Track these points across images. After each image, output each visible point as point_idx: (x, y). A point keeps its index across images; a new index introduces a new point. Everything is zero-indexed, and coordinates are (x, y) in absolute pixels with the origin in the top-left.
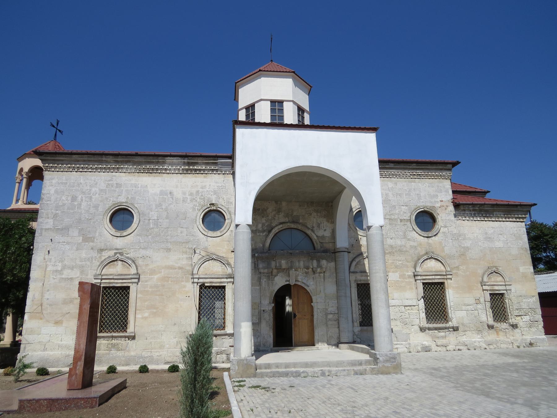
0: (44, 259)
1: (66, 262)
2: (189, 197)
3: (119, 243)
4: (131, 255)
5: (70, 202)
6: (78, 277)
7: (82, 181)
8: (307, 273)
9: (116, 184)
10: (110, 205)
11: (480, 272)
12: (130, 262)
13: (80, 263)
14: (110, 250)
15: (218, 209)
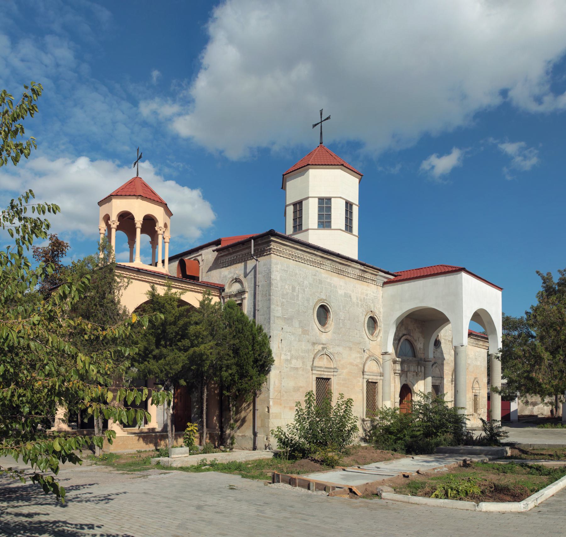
0: (279, 348)
1: (292, 352)
2: (360, 302)
3: (324, 338)
4: (331, 350)
5: (291, 291)
6: (301, 368)
7: (297, 272)
8: (414, 375)
9: (319, 280)
10: (317, 300)
11: (472, 381)
12: (332, 357)
13: (302, 354)
14: (319, 344)
15: (375, 316)
